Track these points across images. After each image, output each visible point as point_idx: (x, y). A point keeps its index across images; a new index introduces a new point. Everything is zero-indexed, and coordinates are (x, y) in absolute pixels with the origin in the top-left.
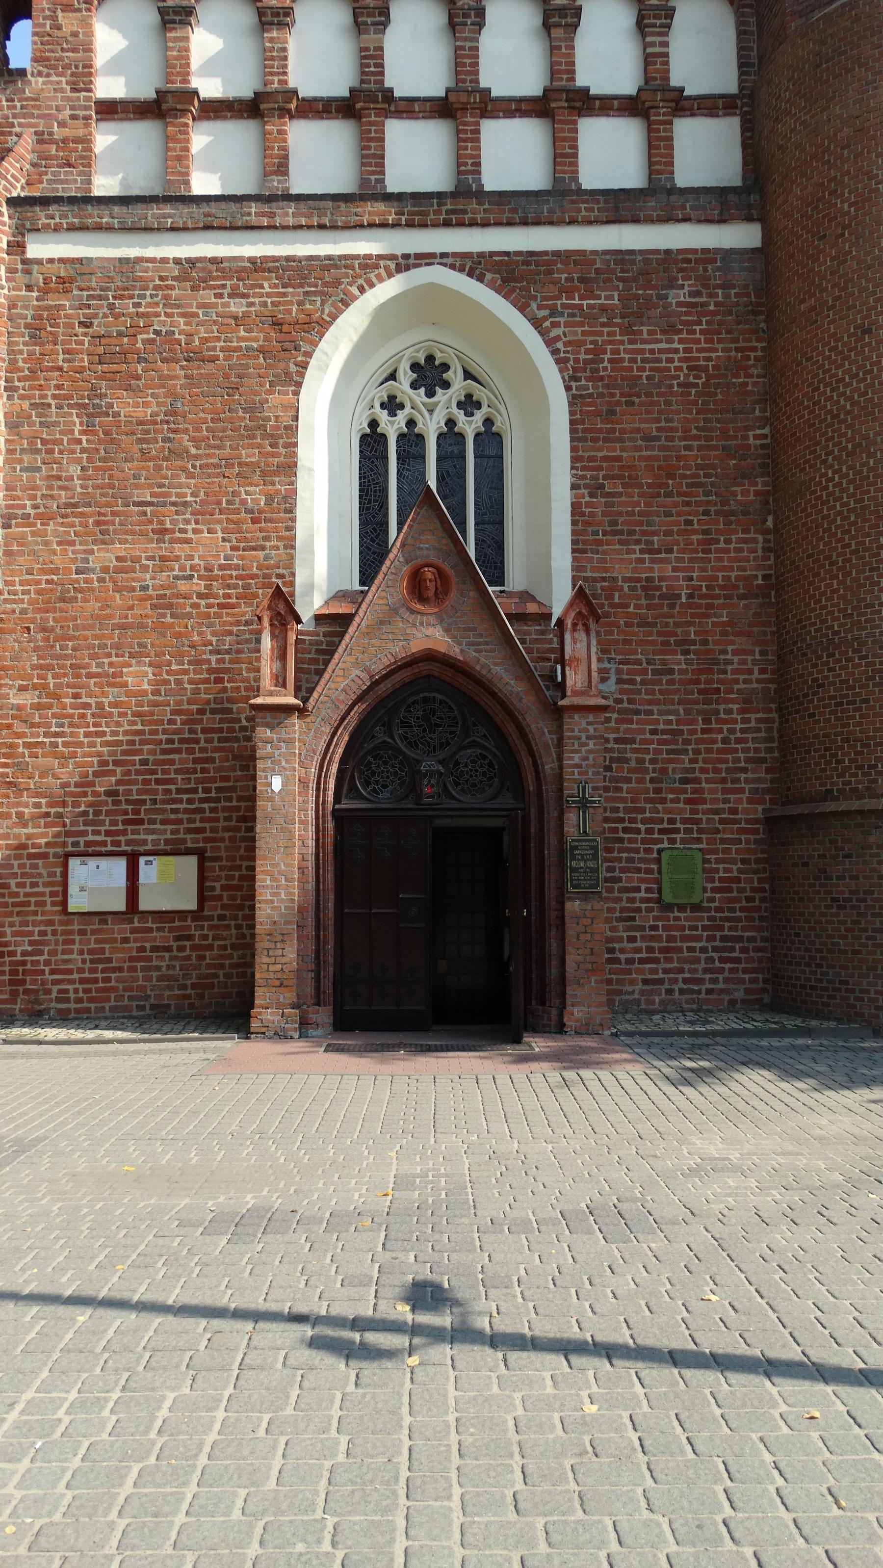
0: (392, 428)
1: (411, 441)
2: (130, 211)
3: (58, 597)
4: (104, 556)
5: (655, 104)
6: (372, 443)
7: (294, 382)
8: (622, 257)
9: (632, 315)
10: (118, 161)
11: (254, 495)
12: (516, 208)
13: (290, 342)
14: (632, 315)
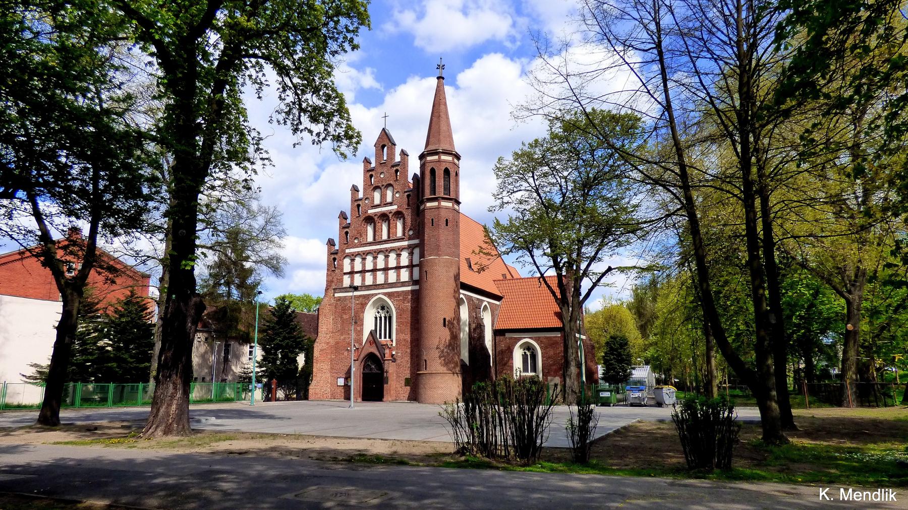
0: (378, 316)
1: (381, 318)
2: (345, 290)
3: (337, 343)
4: (342, 337)
5: (411, 266)
6: (376, 318)
7: (363, 312)
8: (403, 292)
9: (404, 299)
10: (347, 281)
11: (359, 328)
12: (392, 285)
13: (363, 306)
14: (404, 299)
